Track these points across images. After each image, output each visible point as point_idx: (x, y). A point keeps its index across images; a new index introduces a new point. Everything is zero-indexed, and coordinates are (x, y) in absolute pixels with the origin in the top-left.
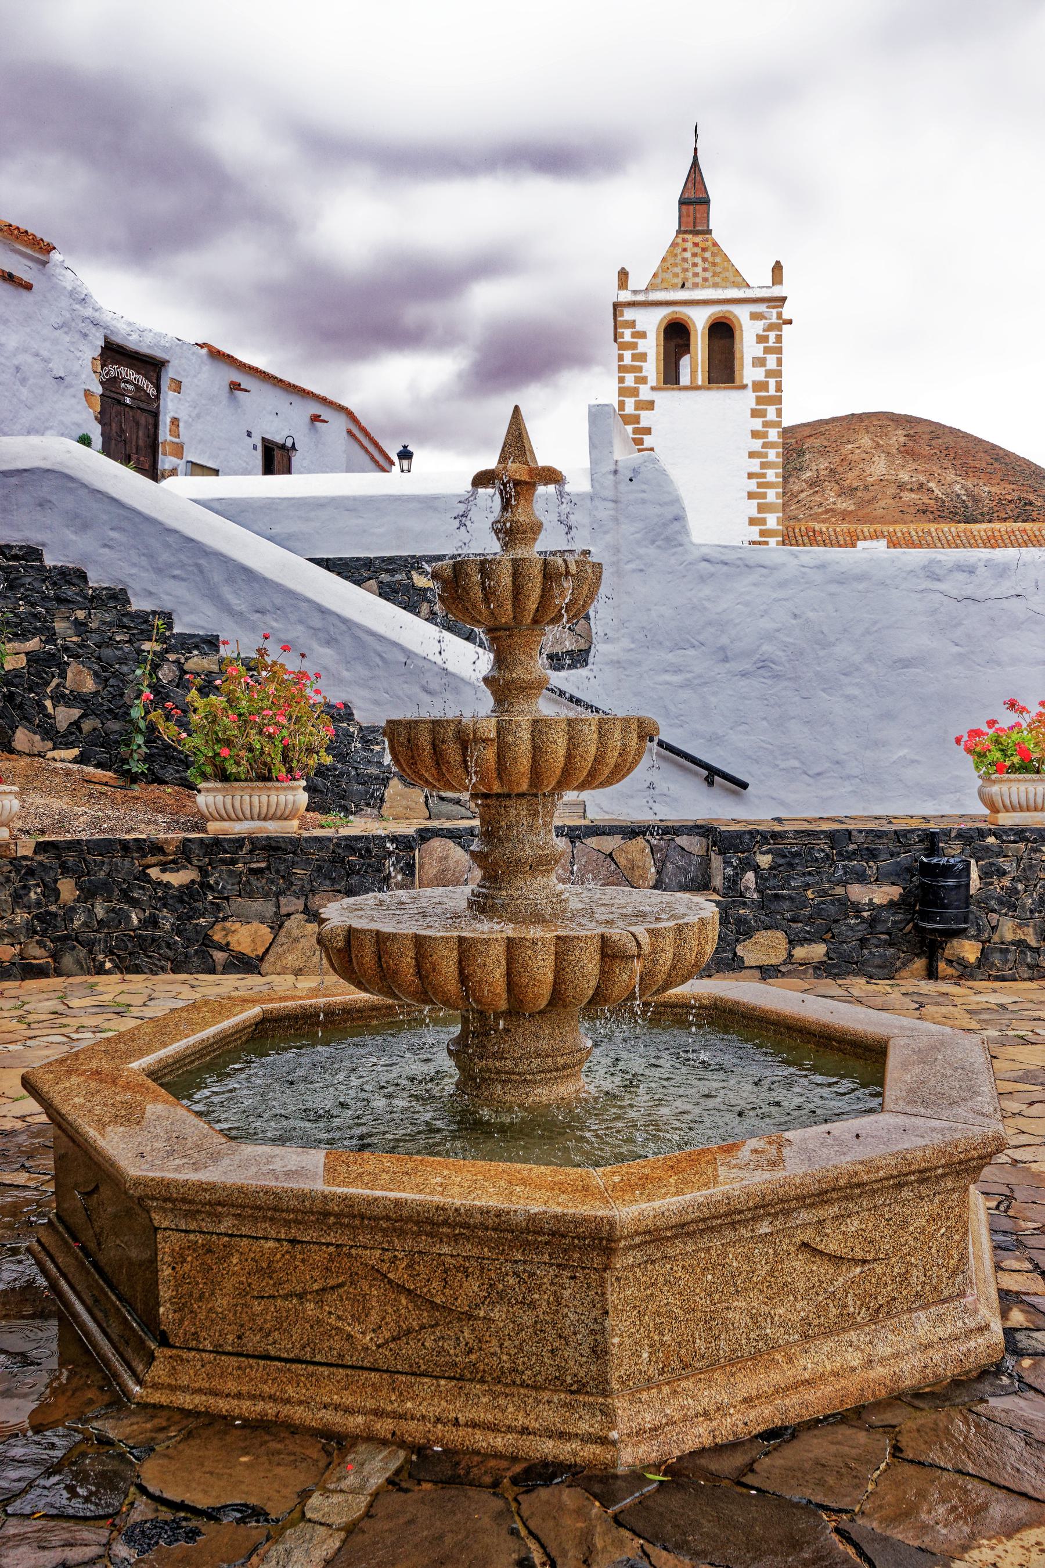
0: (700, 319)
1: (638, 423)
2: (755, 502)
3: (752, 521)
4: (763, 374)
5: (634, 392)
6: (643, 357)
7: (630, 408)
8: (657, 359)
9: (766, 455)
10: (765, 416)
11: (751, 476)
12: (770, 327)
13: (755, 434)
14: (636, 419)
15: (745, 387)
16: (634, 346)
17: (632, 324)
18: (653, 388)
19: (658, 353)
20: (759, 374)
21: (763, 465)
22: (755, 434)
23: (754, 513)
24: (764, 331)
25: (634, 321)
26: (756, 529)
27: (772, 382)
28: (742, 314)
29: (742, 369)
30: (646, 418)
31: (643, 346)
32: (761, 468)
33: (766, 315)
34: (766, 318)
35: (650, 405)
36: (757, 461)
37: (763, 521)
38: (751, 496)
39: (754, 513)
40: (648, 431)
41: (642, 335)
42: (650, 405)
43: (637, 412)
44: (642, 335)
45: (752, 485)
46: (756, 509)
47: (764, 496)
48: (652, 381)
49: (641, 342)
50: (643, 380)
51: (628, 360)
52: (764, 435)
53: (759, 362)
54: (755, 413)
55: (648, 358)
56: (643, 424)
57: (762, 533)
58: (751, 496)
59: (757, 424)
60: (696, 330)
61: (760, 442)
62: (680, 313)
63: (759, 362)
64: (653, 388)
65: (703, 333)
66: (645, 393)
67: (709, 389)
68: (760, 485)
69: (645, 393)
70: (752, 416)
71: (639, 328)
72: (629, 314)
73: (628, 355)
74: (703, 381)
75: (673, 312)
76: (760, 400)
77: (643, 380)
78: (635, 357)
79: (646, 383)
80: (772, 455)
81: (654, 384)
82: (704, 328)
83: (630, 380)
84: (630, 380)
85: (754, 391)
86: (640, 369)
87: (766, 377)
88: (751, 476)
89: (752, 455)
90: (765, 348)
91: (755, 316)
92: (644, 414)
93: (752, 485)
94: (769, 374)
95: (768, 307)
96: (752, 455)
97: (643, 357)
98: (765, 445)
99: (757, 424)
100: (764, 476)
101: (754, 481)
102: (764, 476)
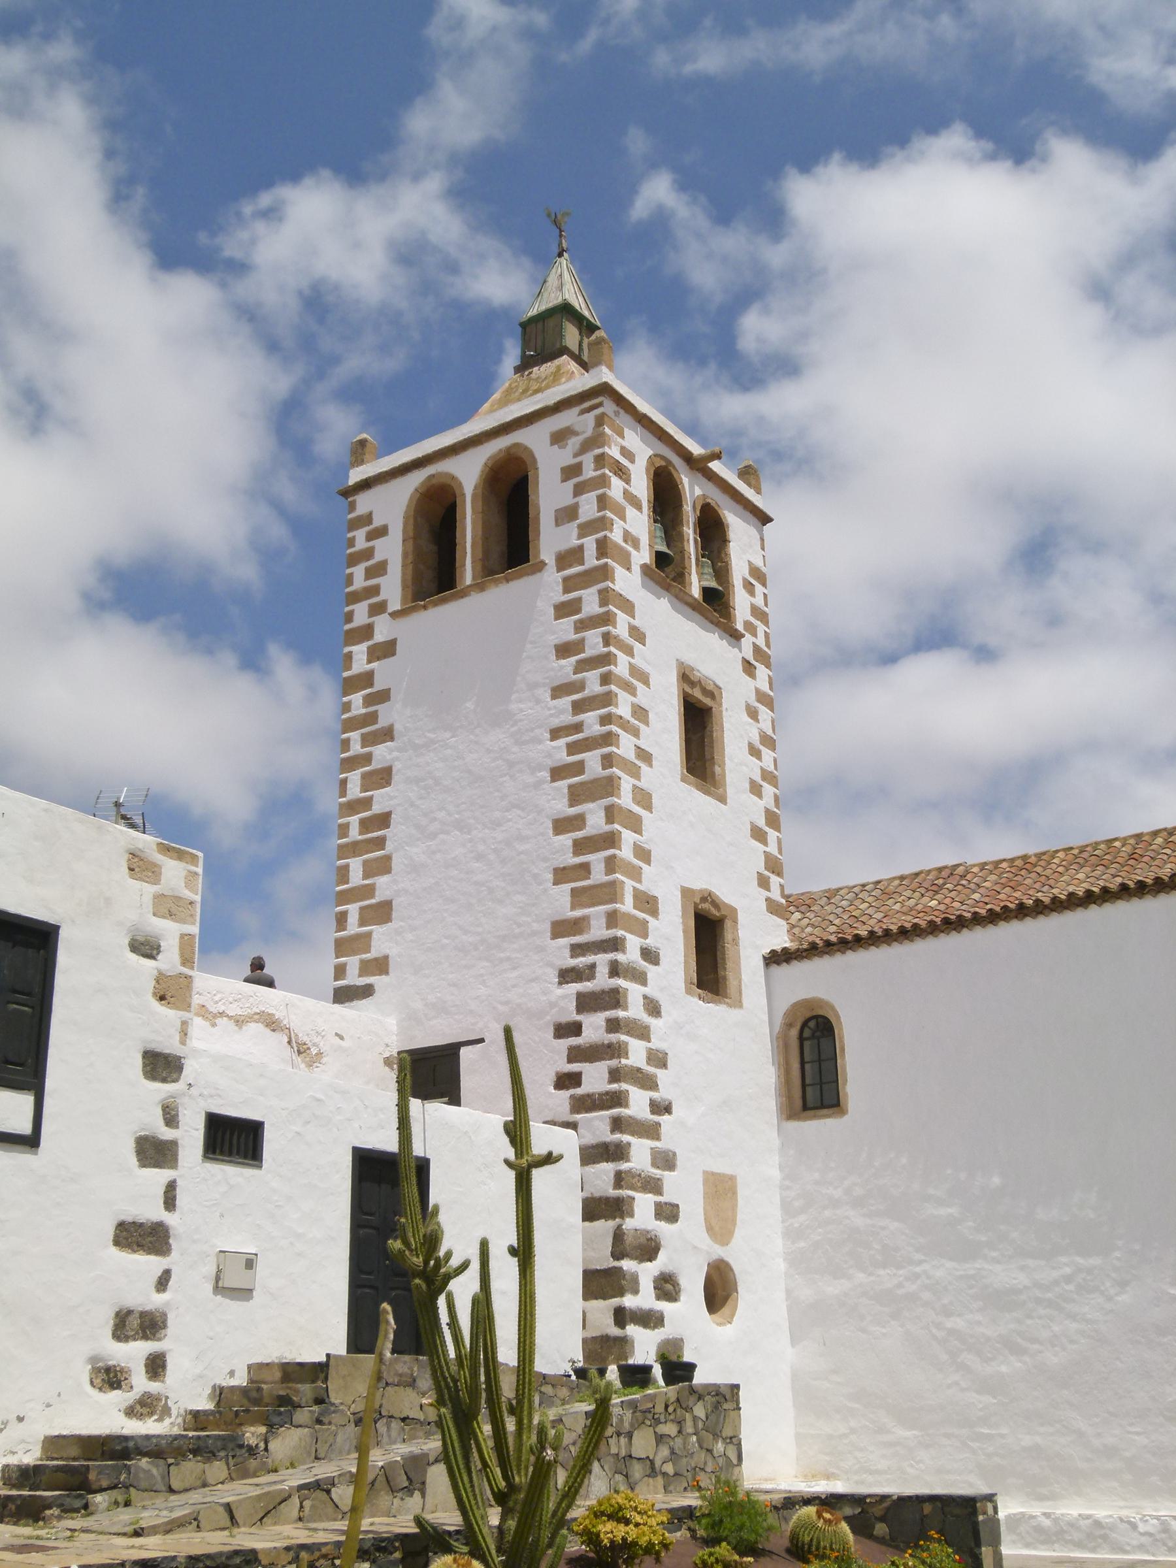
2: (563, 784)
3: (562, 825)
4: (575, 532)
8: (404, 566)
11: (556, 734)
12: (586, 447)
13: (564, 650)
17: (367, 519)
18: (395, 615)
19: (405, 555)
20: (569, 537)
22: (564, 650)
24: (576, 455)
25: (371, 513)
26: (567, 840)
27: (590, 543)
28: (535, 438)
32: (575, 713)
33: (577, 428)
34: (576, 434)
36: (566, 702)
37: (577, 822)
38: (557, 773)
39: (562, 807)
40: (383, 696)
42: (386, 650)
44: (382, 532)
45: (558, 751)
46: (565, 801)
47: (578, 768)
48: (395, 605)
49: (377, 543)
50: (378, 609)
53: (567, 514)
54: (564, 610)
55: (390, 568)
56: (379, 685)
57: (580, 847)
58: (557, 773)
59: (565, 630)
60: (464, 495)
62: (440, 474)
64: (395, 615)
65: (474, 496)
66: (383, 630)
67: (479, 587)
68: (572, 748)
69: (383, 630)
71: (377, 522)
72: (364, 503)
74: (474, 578)
75: (432, 476)
76: (569, 584)
81: (398, 607)
82: (476, 488)
85: (560, 568)
86: (375, 590)
88: (556, 734)
89: (559, 691)
91: (559, 438)
94: (586, 529)
95: (583, 412)
96: (559, 691)
97: (380, 569)
99: (565, 630)
100: (577, 727)
101: (562, 742)
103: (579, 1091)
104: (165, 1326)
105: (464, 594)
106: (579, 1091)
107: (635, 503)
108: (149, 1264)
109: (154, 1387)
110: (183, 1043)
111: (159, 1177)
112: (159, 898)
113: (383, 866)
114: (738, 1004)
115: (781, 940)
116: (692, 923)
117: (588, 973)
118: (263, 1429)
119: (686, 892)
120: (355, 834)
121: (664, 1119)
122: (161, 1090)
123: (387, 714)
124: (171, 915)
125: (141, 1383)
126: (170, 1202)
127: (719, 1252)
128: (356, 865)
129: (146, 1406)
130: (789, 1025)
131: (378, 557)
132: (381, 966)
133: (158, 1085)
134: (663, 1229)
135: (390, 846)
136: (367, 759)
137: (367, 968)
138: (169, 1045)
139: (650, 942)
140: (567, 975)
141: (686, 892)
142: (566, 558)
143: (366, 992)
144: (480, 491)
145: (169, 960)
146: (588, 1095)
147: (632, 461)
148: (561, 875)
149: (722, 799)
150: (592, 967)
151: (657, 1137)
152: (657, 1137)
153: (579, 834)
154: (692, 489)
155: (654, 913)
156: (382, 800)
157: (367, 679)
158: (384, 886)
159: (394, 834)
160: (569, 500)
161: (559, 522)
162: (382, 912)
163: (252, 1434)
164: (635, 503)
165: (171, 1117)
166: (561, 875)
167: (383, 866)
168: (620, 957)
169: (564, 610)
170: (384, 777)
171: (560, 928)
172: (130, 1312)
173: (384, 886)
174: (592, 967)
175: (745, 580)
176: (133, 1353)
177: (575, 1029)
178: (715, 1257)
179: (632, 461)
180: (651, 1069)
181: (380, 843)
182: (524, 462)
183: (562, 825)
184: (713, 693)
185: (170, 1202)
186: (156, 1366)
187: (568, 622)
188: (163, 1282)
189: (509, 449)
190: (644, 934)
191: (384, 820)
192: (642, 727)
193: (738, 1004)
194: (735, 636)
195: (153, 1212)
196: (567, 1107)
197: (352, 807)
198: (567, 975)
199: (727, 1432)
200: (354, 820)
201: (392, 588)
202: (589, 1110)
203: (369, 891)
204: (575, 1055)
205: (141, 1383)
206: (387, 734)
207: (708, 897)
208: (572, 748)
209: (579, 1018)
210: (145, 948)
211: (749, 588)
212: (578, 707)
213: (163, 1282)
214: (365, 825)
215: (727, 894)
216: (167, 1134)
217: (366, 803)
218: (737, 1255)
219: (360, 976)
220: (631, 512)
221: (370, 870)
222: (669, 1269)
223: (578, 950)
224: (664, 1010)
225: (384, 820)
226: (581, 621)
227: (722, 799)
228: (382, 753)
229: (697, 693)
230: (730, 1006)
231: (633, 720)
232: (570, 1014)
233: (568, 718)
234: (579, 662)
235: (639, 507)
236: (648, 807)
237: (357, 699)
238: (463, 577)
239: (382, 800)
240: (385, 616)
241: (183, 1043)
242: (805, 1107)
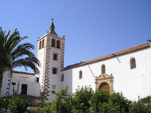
53: (45, 43)
107: (50, 42)
119: (52, 68)
149: (57, 61)
154: (56, 39)
165: (10, 83)
169: (45, 50)
188: (9, 90)
211: (62, 45)
213: (9, 90)
220: (49, 43)
227: (57, 61)
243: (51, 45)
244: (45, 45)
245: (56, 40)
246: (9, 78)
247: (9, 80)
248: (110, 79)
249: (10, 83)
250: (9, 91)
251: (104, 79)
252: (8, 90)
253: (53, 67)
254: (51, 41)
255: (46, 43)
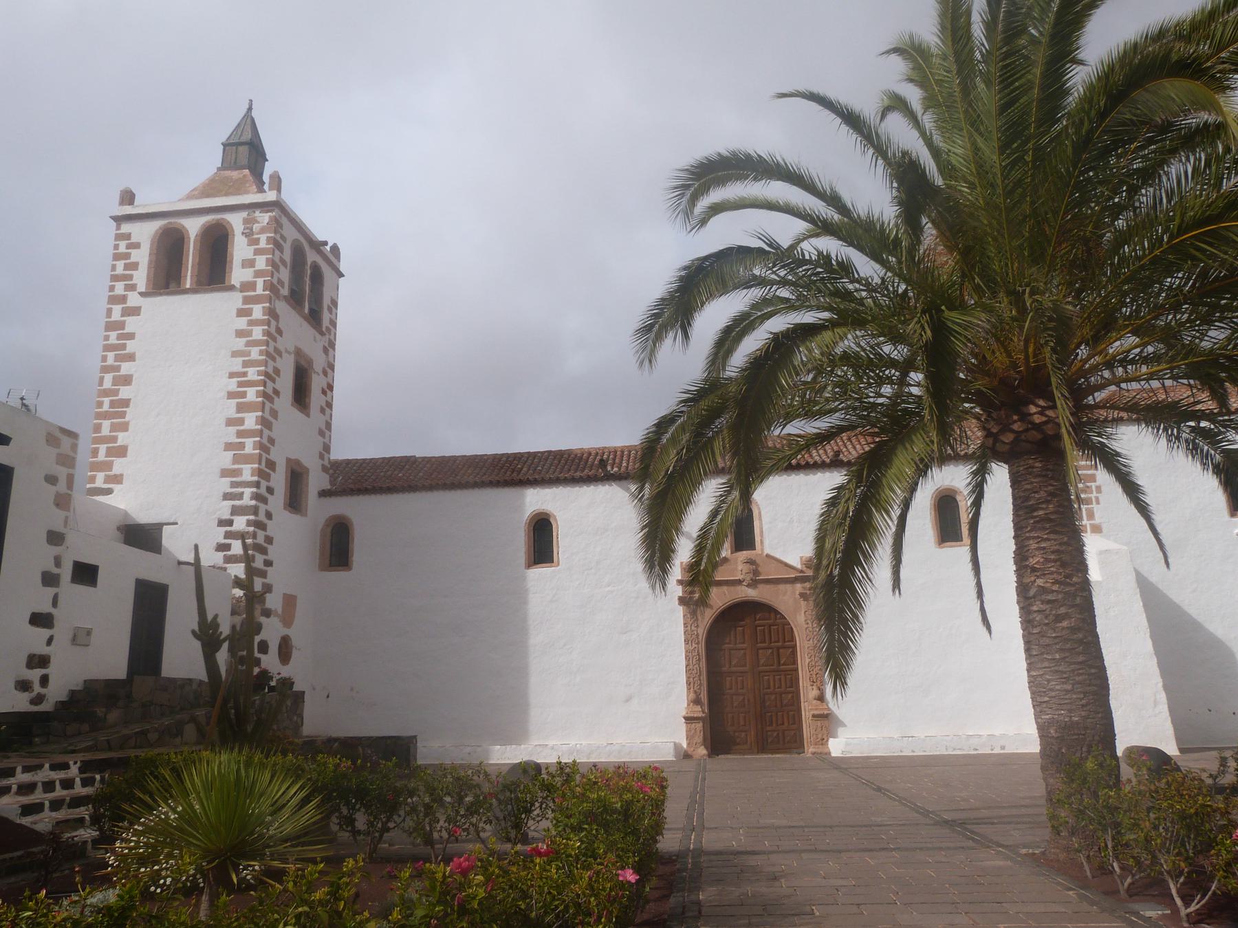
0: (193, 227)
1: (123, 329)
3: (230, 422)
5: (123, 299)
6: (134, 266)
7: (116, 315)
9: (249, 354)
10: (250, 315)
11: (232, 375)
13: (240, 334)
14: (121, 325)
15: (232, 288)
16: (127, 256)
17: (127, 236)
18: (141, 294)
19: (150, 262)
21: (246, 364)
22: (240, 334)
23: (232, 412)
25: (130, 234)
28: (236, 221)
29: (231, 272)
30: (132, 324)
31: (136, 256)
32: (244, 367)
33: (259, 219)
34: (259, 223)
35: (135, 311)
36: (240, 360)
37: (241, 421)
38: (231, 395)
40: (131, 336)
41: (137, 246)
42: (135, 311)
43: (123, 319)
44: (137, 246)
47: (244, 395)
48: (142, 287)
49: (134, 252)
50: (132, 288)
51: (120, 270)
52: (248, 334)
53: (248, 263)
54: (241, 313)
57: (240, 434)
58: (231, 395)
60: (189, 238)
61: (244, 340)
63: (248, 263)
66: (134, 300)
67: (193, 291)
68: (240, 384)
69: (134, 300)
70: (238, 316)
71: (133, 240)
72: (126, 228)
73: (120, 265)
74: (191, 284)
75: (170, 223)
76: (247, 300)
77: (132, 288)
78: (127, 267)
79: (135, 290)
80: (255, 353)
81: (143, 289)
83: (120, 288)
84: (120, 288)
86: (130, 277)
87: (255, 277)
88: (232, 375)
89: (235, 354)
90: (255, 250)
92: (128, 319)
93: (232, 385)
96: (235, 354)
97: (134, 266)
98: (249, 344)
100: (245, 374)
101: (235, 380)
102: (245, 374)
103: (229, 553)
104: (49, 662)
105: (186, 292)
106: (229, 553)
108: (45, 633)
109: (43, 691)
110: (65, 526)
111: (51, 591)
112: (59, 455)
113: (124, 427)
114: (306, 515)
115: (327, 486)
116: (289, 475)
117: (240, 496)
118: (104, 710)
119: (289, 460)
120: (106, 407)
121: (269, 569)
122: (56, 550)
123: (131, 346)
124: (63, 464)
125: (37, 689)
126: (55, 603)
127: (285, 631)
128: (106, 425)
129: (39, 699)
130: (327, 524)
131: (133, 259)
132: (118, 479)
133: (54, 547)
134: (263, 619)
135: (127, 419)
136: (118, 369)
137: (108, 480)
138: (59, 528)
139: (271, 484)
140: (227, 496)
141: (289, 460)
142: (248, 286)
143: (109, 492)
144: (199, 238)
145: (62, 487)
146: (234, 555)
147: (285, 242)
148: (229, 446)
149: (308, 415)
150: (242, 493)
151: (265, 577)
152: (265, 577)
153: (242, 428)
154: (311, 257)
155: (274, 470)
156: (125, 392)
157: (121, 325)
158: (122, 439)
159: (131, 414)
160: (250, 256)
161: (243, 266)
162: (122, 452)
163: (100, 711)
164: (283, 262)
166: (229, 446)
167: (124, 427)
168: (254, 490)
169: (241, 313)
170: (127, 380)
171: (225, 473)
172: (34, 655)
173: (122, 439)
174: (242, 493)
175: (328, 306)
176: (35, 675)
177: (230, 523)
178: (283, 634)
179: (285, 242)
180: (266, 545)
181: (123, 415)
182: (224, 226)
183: (230, 422)
184: (310, 362)
185: (55, 603)
186: (44, 680)
187: (245, 320)
189: (218, 220)
190: (268, 481)
191: (126, 403)
192: (277, 378)
193: (306, 515)
194: (322, 334)
195: (46, 608)
196: (222, 561)
197: (106, 393)
198: (227, 496)
199: (298, 712)
200: (106, 401)
201: (141, 278)
202: (235, 562)
203: (115, 439)
204: (228, 535)
205: (37, 689)
206: (131, 357)
207: (297, 462)
208: (240, 384)
209: (232, 518)
210: (51, 480)
212: (246, 364)
214: (112, 404)
215: (306, 462)
216: (55, 571)
217: (116, 393)
218: (293, 633)
219: (104, 483)
220: (282, 268)
221: (114, 428)
222: (265, 638)
223: (234, 484)
224: (274, 517)
225: (126, 403)
226: (251, 320)
227: (308, 415)
228: (126, 368)
229: (303, 363)
230: (302, 515)
231: (273, 375)
232: (226, 516)
233: (239, 368)
234: (248, 341)
235: (286, 267)
236: (276, 418)
237: (113, 335)
238: (185, 283)
239: (125, 392)
240: (136, 293)
241: (65, 526)
242: (331, 565)
243: (285, 291)
244: (238, 275)
245: (309, 263)
246: (54, 507)
247: (55, 538)
248: (798, 586)
249: (58, 562)
250: (44, 650)
251: (754, 583)
252: (36, 639)
253: (293, 457)
254: (287, 256)
255: (261, 263)
